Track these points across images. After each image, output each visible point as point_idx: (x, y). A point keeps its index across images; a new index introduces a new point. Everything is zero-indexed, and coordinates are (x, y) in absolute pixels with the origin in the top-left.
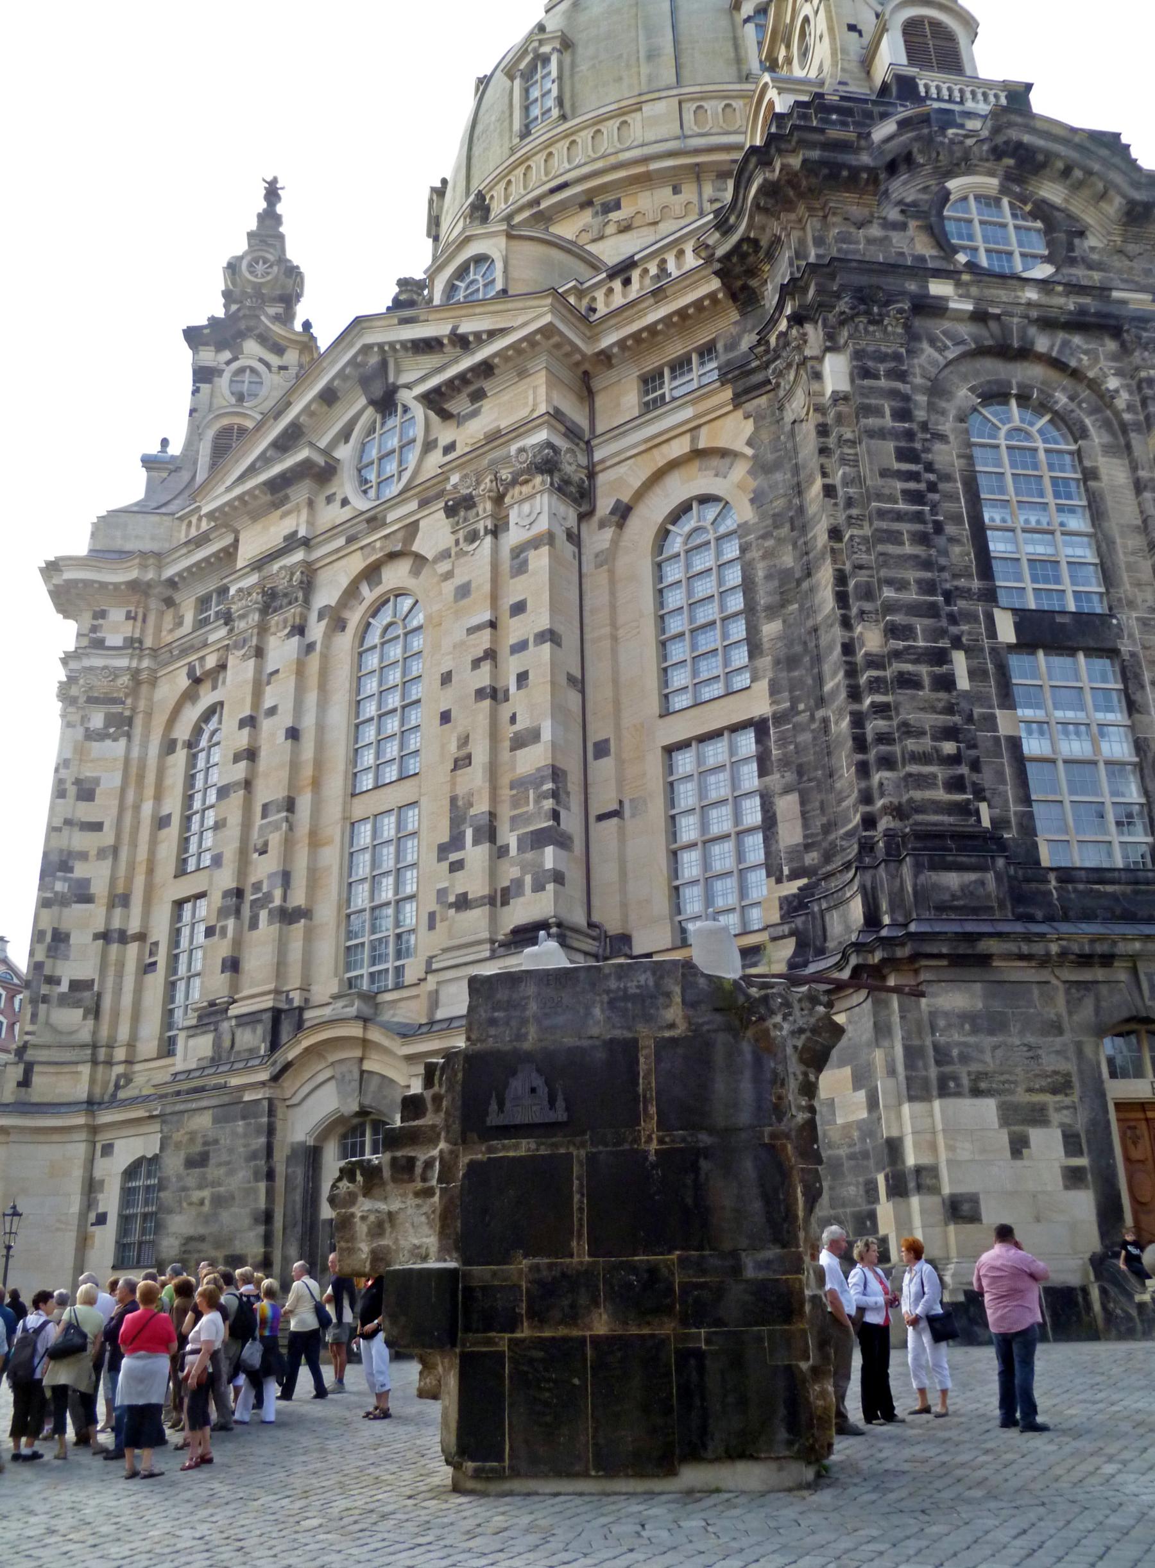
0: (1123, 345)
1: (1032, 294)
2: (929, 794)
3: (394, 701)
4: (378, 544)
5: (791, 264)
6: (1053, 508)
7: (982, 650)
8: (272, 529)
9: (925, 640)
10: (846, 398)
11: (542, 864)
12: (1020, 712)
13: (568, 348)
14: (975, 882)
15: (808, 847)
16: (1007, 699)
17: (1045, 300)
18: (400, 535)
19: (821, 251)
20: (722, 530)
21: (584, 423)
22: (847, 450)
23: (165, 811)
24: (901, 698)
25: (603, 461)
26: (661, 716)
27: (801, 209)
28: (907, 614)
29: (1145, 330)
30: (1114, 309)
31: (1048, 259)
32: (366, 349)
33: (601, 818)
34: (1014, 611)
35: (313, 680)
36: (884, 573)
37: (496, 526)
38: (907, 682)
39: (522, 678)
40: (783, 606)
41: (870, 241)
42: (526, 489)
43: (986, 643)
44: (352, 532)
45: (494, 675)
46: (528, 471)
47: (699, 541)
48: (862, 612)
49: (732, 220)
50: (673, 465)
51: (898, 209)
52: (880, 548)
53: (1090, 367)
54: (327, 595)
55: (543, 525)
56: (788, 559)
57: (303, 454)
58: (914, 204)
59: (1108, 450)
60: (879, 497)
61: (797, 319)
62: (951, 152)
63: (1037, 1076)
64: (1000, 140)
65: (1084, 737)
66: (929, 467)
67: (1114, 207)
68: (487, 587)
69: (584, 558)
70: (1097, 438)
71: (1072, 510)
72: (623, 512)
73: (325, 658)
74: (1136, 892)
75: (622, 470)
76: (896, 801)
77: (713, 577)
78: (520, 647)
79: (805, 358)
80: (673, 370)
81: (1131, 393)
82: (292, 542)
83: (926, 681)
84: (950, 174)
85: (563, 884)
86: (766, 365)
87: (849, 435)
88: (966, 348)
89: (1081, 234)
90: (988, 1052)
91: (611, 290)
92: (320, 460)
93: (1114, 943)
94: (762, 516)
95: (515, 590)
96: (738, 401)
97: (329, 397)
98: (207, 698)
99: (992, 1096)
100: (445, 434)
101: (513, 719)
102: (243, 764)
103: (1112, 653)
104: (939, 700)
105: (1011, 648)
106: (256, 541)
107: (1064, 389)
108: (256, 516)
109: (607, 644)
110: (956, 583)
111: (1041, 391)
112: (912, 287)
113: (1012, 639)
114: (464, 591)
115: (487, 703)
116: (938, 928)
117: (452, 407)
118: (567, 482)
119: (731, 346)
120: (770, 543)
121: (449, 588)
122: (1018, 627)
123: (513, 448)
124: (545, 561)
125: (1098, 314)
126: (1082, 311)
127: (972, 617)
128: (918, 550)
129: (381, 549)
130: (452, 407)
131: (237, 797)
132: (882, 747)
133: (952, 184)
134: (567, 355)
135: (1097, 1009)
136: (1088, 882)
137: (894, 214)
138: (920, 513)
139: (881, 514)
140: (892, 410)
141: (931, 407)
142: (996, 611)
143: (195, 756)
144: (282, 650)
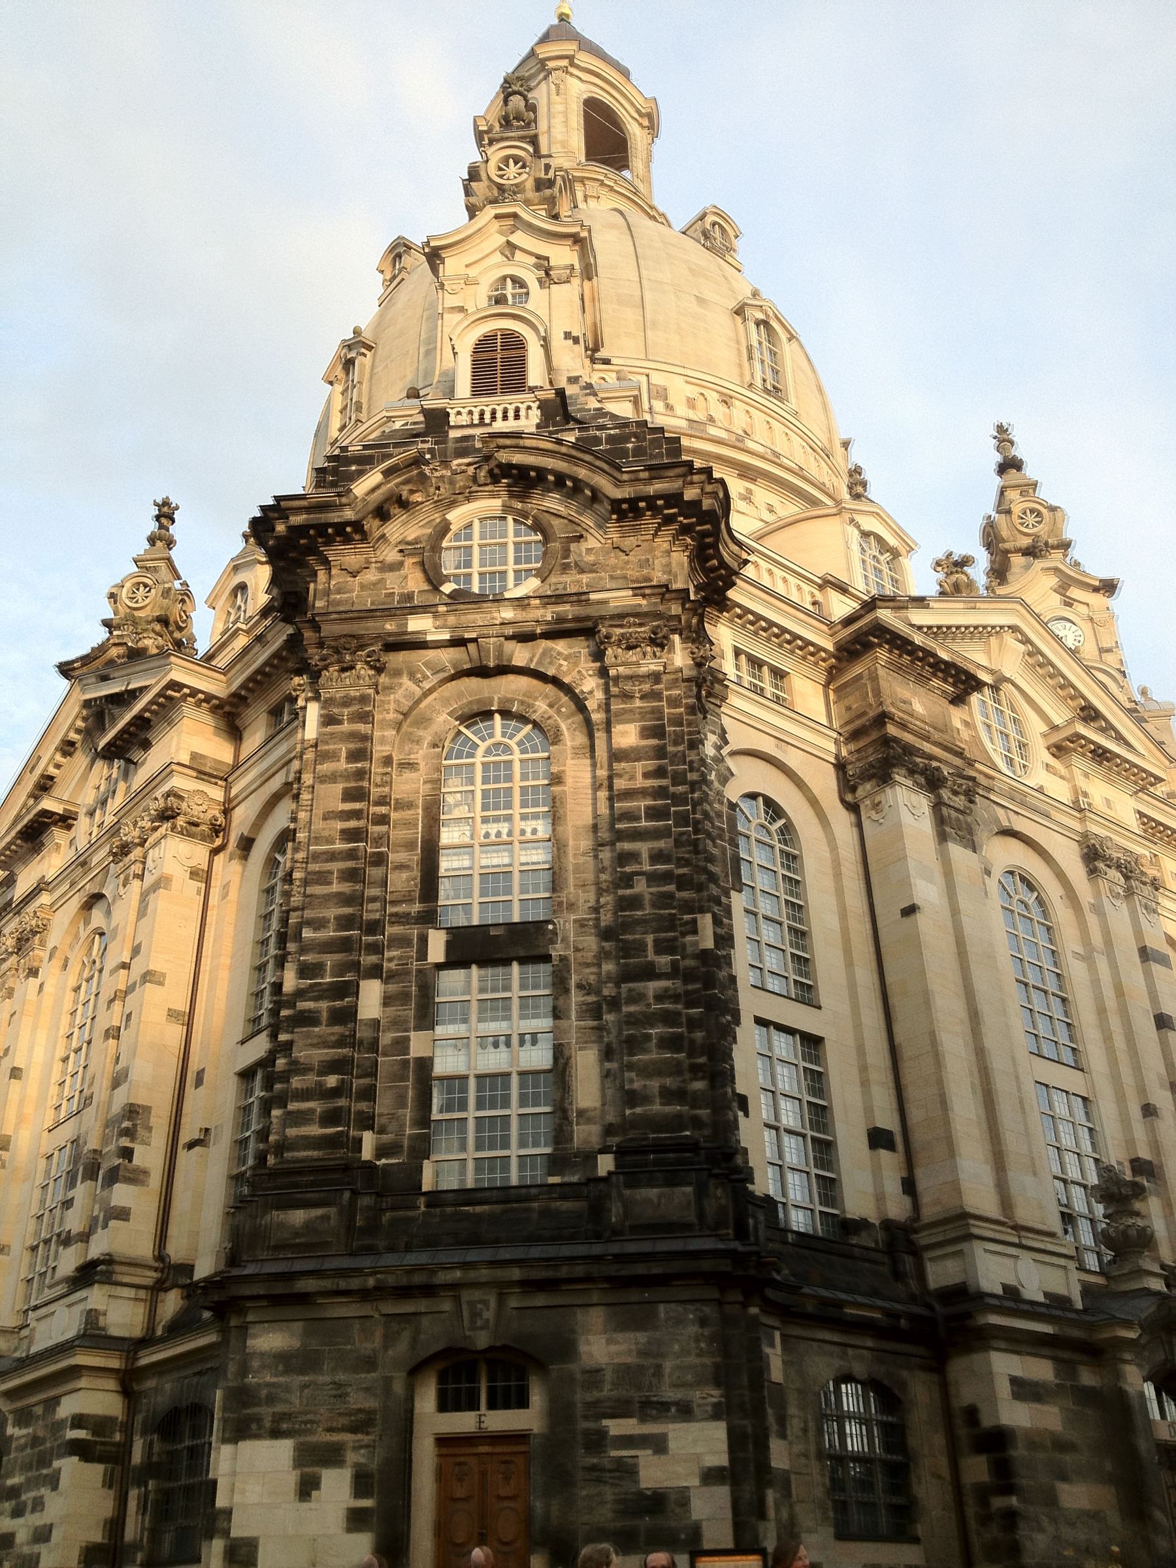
1: (508, 614)
6: (517, 817)
11: (109, 1200)
12: (440, 1030)
16: (426, 1017)
17: (520, 615)
24: (295, 1037)
25: (236, 796)
29: (621, 626)
32: (87, 704)
33: (191, 1145)
36: (309, 914)
38: (307, 1019)
41: (363, 587)
52: (309, 890)
53: (569, 672)
58: (417, 541)
60: (318, 840)
62: (452, 483)
63: (340, 1414)
64: (493, 463)
71: (535, 816)
72: (246, 844)
84: (452, 504)
85: (128, 1220)
88: (446, 675)
90: (296, 1394)
93: (433, 1272)
99: (292, 1437)
104: (333, 1034)
105: (439, 967)
107: (546, 696)
111: (522, 703)
112: (390, 626)
122: (449, 945)
125: (577, 619)
126: (560, 619)
127: (403, 942)
128: (346, 888)
133: (450, 516)
135: (414, 1341)
137: (392, 555)
138: (355, 849)
139: (316, 857)
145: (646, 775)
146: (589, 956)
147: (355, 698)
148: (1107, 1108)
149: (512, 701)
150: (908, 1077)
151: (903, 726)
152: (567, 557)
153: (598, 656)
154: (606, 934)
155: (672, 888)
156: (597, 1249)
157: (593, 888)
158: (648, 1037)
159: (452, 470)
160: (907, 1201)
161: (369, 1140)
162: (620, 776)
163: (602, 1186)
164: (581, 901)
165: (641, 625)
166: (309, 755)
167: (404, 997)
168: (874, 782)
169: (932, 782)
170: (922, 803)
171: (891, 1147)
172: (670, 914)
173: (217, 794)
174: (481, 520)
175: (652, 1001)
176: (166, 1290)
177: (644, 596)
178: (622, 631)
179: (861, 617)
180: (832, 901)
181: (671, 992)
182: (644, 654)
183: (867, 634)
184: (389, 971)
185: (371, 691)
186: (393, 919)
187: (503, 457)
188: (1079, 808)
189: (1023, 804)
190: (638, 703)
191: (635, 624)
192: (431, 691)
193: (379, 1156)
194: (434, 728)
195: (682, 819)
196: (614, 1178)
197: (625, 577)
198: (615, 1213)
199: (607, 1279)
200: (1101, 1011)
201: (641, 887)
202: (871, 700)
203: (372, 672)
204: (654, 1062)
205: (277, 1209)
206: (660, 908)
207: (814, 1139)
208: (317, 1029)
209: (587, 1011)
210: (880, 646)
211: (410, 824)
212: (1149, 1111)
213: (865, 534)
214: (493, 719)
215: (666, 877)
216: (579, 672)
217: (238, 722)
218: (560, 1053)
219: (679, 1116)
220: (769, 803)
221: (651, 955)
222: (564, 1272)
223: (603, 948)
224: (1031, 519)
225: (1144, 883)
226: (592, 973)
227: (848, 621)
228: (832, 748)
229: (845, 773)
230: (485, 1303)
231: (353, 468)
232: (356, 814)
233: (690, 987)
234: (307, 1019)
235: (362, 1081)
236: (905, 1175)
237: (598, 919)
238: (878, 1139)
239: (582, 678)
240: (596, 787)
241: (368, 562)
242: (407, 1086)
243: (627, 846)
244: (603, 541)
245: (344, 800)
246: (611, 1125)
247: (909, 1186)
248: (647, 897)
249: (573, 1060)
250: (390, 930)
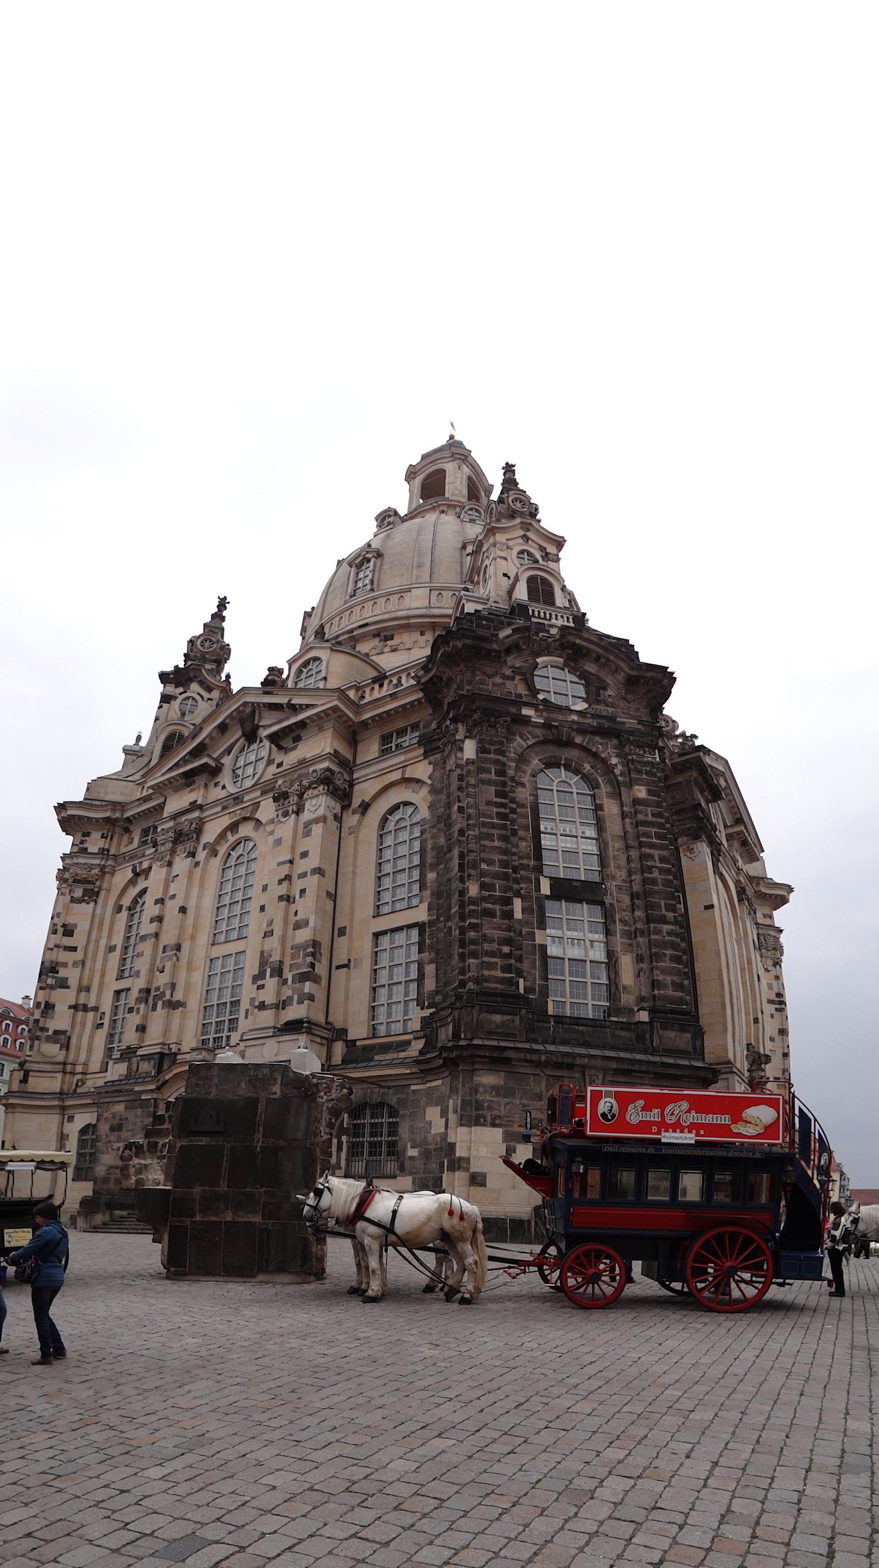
0: (620, 742)
2: (492, 973)
3: (239, 896)
4: (238, 812)
5: (455, 692)
7: (532, 897)
8: (185, 798)
10: (473, 762)
12: (548, 931)
13: (345, 718)
15: (437, 993)
18: (250, 808)
19: (469, 688)
20: (414, 821)
21: (350, 758)
22: (471, 790)
23: (113, 943)
25: (357, 779)
26: (374, 917)
27: (462, 666)
28: (492, 878)
34: (551, 878)
35: (196, 883)
37: (298, 809)
38: (490, 913)
39: (303, 891)
40: (438, 865)
42: (316, 792)
44: (225, 804)
45: (289, 889)
46: (316, 782)
47: (402, 825)
48: (469, 875)
49: (430, 666)
50: (392, 785)
52: (482, 842)
54: (210, 834)
55: (321, 812)
56: (442, 841)
57: (205, 760)
59: (610, 795)
60: (484, 816)
61: (454, 721)
66: (513, 800)
68: (290, 842)
69: (343, 829)
70: (604, 789)
72: (365, 807)
73: (204, 869)
75: (366, 784)
76: (476, 975)
77: (406, 847)
78: (303, 875)
79: (455, 740)
80: (398, 734)
81: (623, 766)
82: (194, 806)
83: (498, 913)
86: (440, 739)
87: (472, 782)
91: (373, 688)
92: (213, 764)
94: (433, 816)
95: (305, 844)
96: (426, 755)
97: (223, 728)
98: (141, 884)
100: (278, 757)
101: (296, 914)
102: (155, 924)
103: (602, 903)
105: (547, 897)
106: (176, 803)
107: (589, 762)
108: (176, 790)
109: (350, 876)
110: (521, 862)
113: (549, 893)
114: (278, 842)
115: (284, 903)
116: (487, 1043)
117: (283, 744)
118: (336, 789)
119: (427, 726)
120: (435, 831)
121: (271, 839)
123: (311, 769)
124: (320, 831)
125: (609, 728)
129: (240, 815)
130: (283, 744)
131: (150, 942)
132: (472, 947)
134: (345, 722)
139: (484, 824)
140: (495, 769)
141: (518, 768)
142: (541, 877)
143: (132, 915)
144: (181, 864)
149: (572, 761)
153: (621, 746)
154: (633, 896)
162: (640, 813)
173: (347, 777)
190: (644, 776)
194: (532, 766)
202: (688, 796)
218: (610, 954)
232: (504, 805)
237: (631, 887)
239: (611, 757)
240: (623, 816)
241: (497, 672)
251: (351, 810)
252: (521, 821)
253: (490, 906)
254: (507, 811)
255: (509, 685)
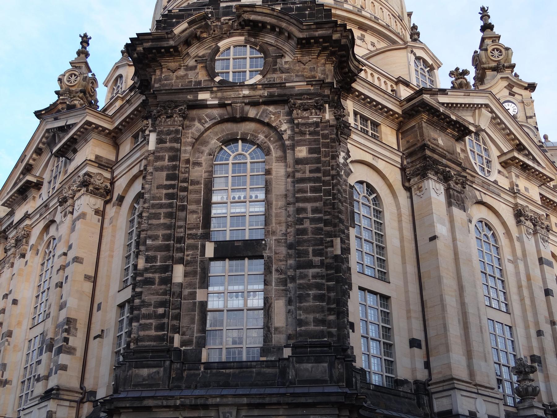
1: (246, 92)
4: (48, 217)
6: (248, 189)
7: (196, 262)
9: (161, 262)
11: (57, 361)
12: (211, 289)
14: (155, 372)
16: (205, 283)
17: (252, 93)
25: (116, 176)
29: (301, 99)
30: (287, 92)
31: (262, 73)
32: (48, 131)
36: (150, 233)
38: (149, 282)
41: (177, 78)
43: (199, 258)
51: (194, 60)
52: (150, 222)
54: (33, 240)
58: (203, 56)
59: (278, 159)
60: (154, 198)
62: (221, 28)
64: (241, 20)
65: (240, 298)
67: (293, 42)
70: (275, 153)
72: (121, 199)
74: (240, 373)
84: (221, 39)
85: (66, 371)
88: (216, 121)
89: (282, 56)
92: (34, 180)
93: (207, 399)
104: (161, 289)
105: (211, 259)
107: (264, 132)
112: (190, 97)
116: (131, 395)
122: (216, 250)
125: (279, 95)
126: (271, 95)
127: (195, 247)
128: (167, 221)
133: (220, 44)
136: (218, 369)
137: (191, 62)
138: (172, 203)
139: (153, 206)
145: (311, 172)
146: (282, 256)
147: (172, 131)
148: (520, 331)
149: (247, 134)
150: (428, 316)
151: (433, 151)
152: (276, 65)
153: (290, 113)
154: (290, 246)
155: (322, 225)
156: (282, 391)
157: (284, 225)
158: (308, 295)
159: (221, 22)
160: (426, 371)
161: (177, 339)
162: (298, 171)
163: (285, 362)
164: (278, 230)
165: (310, 99)
166: (151, 158)
167: (195, 273)
168: (419, 177)
169: (446, 178)
170: (441, 188)
171: (419, 347)
172: (321, 238)
173: (108, 175)
174: (235, 47)
175: (311, 278)
176: (84, 403)
177: (312, 85)
178: (301, 102)
179: (416, 98)
180: (397, 233)
181: (320, 274)
182: (311, 113)
183: (418, 106)
184: (187, 261)
185: (181, 128)
186: (189, 237)
187: (246, 16)
188: (514, 191)
189: (488, 190)
190: (308, 137)
191: (307, 99)
192: (209, 128)
193: (182, 346)
195: (328, 193)
196: (291, 359)
197: (303, 76)
198: (291, 374)
199: (288, 404)
200: (520, 287)
201: (307, 224)
202: (419, 138)
203: (181, 119)
204: (310, 306)
205: (135, 368)
206: (315, 235)
207: (384, 343)
208: (153, 287)
209: (280, 282)
210: (424, 112)
211: (198, 192)
212: (540, 333)
213: (418, 58)
214: (238, 143)
215: (319, 220)
216: (280, 121)
217: (118, 141)
218: (266, 300)
219: (322, 331)
220: (369, 186)
221: (311, 257)
222: (267, 400)
223: (288, 252)
224: (496, 53)
225: (543, 228)
226: (284, 265)
227: (409, 99)
228: (399, 160)
229: (405, 173)
230: (231, 413)
231: (174, 20)
232: (172, 187)
233: (329, 272)
234: (149, 282)
235: (174, 311)
236: (426, 360)
237: (286, 239)
238: (414, 343)
239: (281, 124)
242: (195, 314)
243: (301, 205)
244: (293, 58)
245: (167, 180)
246: (290, 334)
247: (427, 365)
248: (310, 229)
249: (273, 305)
250: (188, 242)
251: (112, 203)
252: (192, 197)
253: (151, 275)
254: (175, 191)
255: (191, 75)
